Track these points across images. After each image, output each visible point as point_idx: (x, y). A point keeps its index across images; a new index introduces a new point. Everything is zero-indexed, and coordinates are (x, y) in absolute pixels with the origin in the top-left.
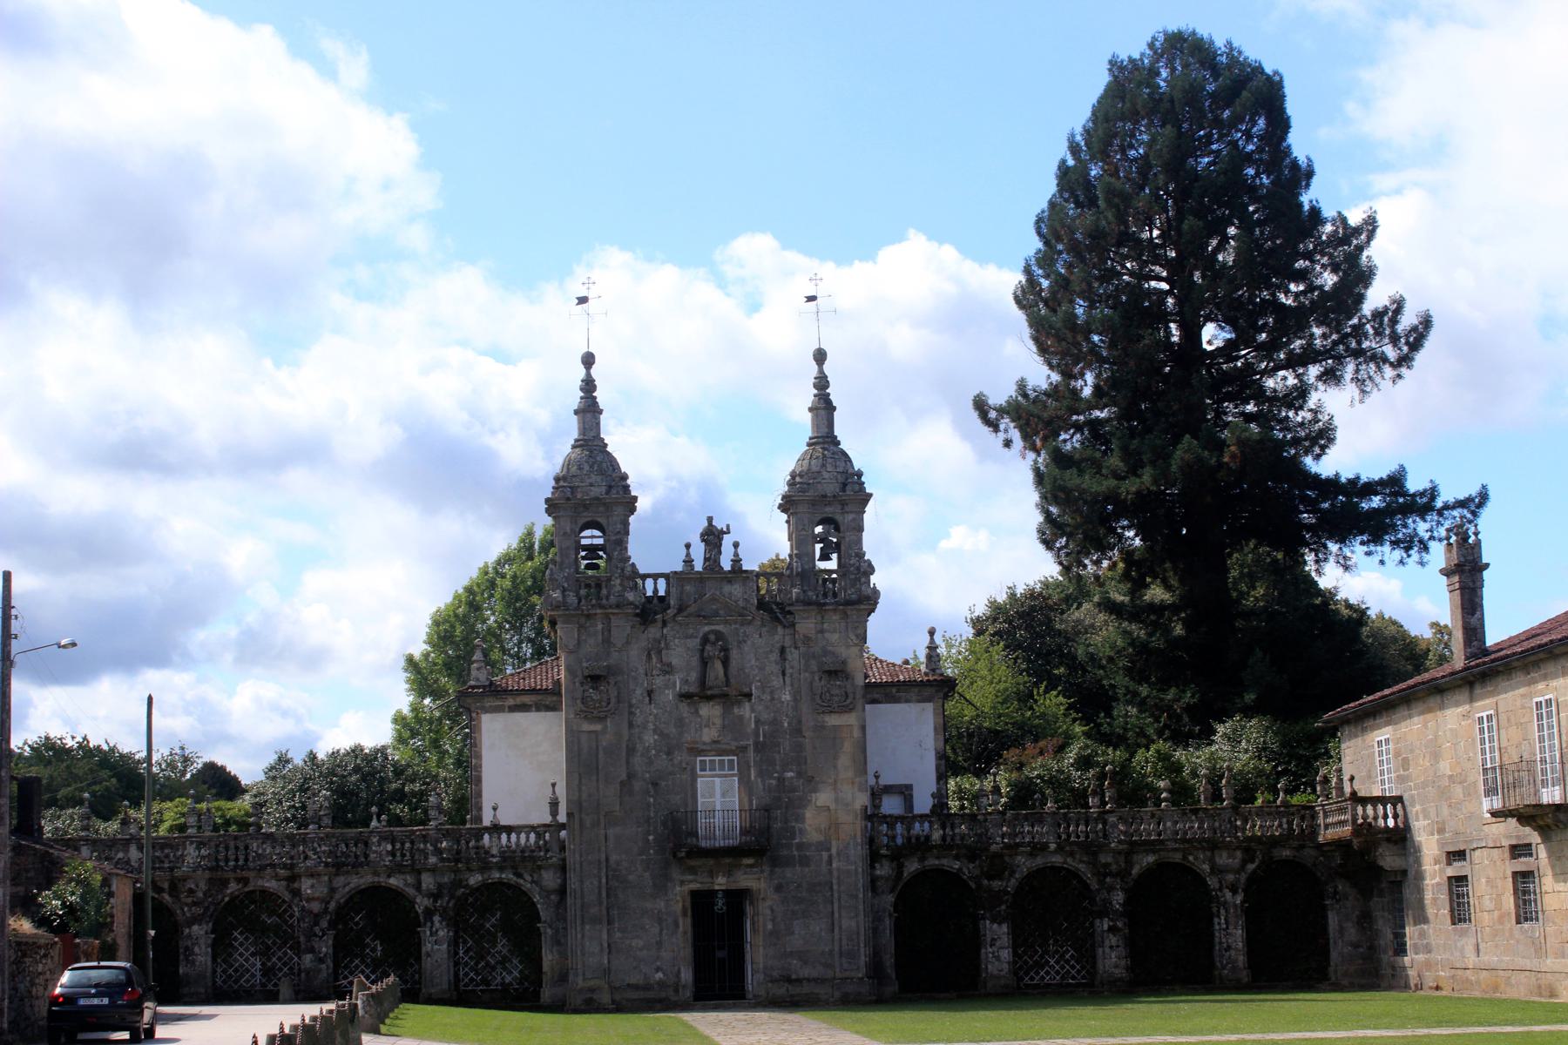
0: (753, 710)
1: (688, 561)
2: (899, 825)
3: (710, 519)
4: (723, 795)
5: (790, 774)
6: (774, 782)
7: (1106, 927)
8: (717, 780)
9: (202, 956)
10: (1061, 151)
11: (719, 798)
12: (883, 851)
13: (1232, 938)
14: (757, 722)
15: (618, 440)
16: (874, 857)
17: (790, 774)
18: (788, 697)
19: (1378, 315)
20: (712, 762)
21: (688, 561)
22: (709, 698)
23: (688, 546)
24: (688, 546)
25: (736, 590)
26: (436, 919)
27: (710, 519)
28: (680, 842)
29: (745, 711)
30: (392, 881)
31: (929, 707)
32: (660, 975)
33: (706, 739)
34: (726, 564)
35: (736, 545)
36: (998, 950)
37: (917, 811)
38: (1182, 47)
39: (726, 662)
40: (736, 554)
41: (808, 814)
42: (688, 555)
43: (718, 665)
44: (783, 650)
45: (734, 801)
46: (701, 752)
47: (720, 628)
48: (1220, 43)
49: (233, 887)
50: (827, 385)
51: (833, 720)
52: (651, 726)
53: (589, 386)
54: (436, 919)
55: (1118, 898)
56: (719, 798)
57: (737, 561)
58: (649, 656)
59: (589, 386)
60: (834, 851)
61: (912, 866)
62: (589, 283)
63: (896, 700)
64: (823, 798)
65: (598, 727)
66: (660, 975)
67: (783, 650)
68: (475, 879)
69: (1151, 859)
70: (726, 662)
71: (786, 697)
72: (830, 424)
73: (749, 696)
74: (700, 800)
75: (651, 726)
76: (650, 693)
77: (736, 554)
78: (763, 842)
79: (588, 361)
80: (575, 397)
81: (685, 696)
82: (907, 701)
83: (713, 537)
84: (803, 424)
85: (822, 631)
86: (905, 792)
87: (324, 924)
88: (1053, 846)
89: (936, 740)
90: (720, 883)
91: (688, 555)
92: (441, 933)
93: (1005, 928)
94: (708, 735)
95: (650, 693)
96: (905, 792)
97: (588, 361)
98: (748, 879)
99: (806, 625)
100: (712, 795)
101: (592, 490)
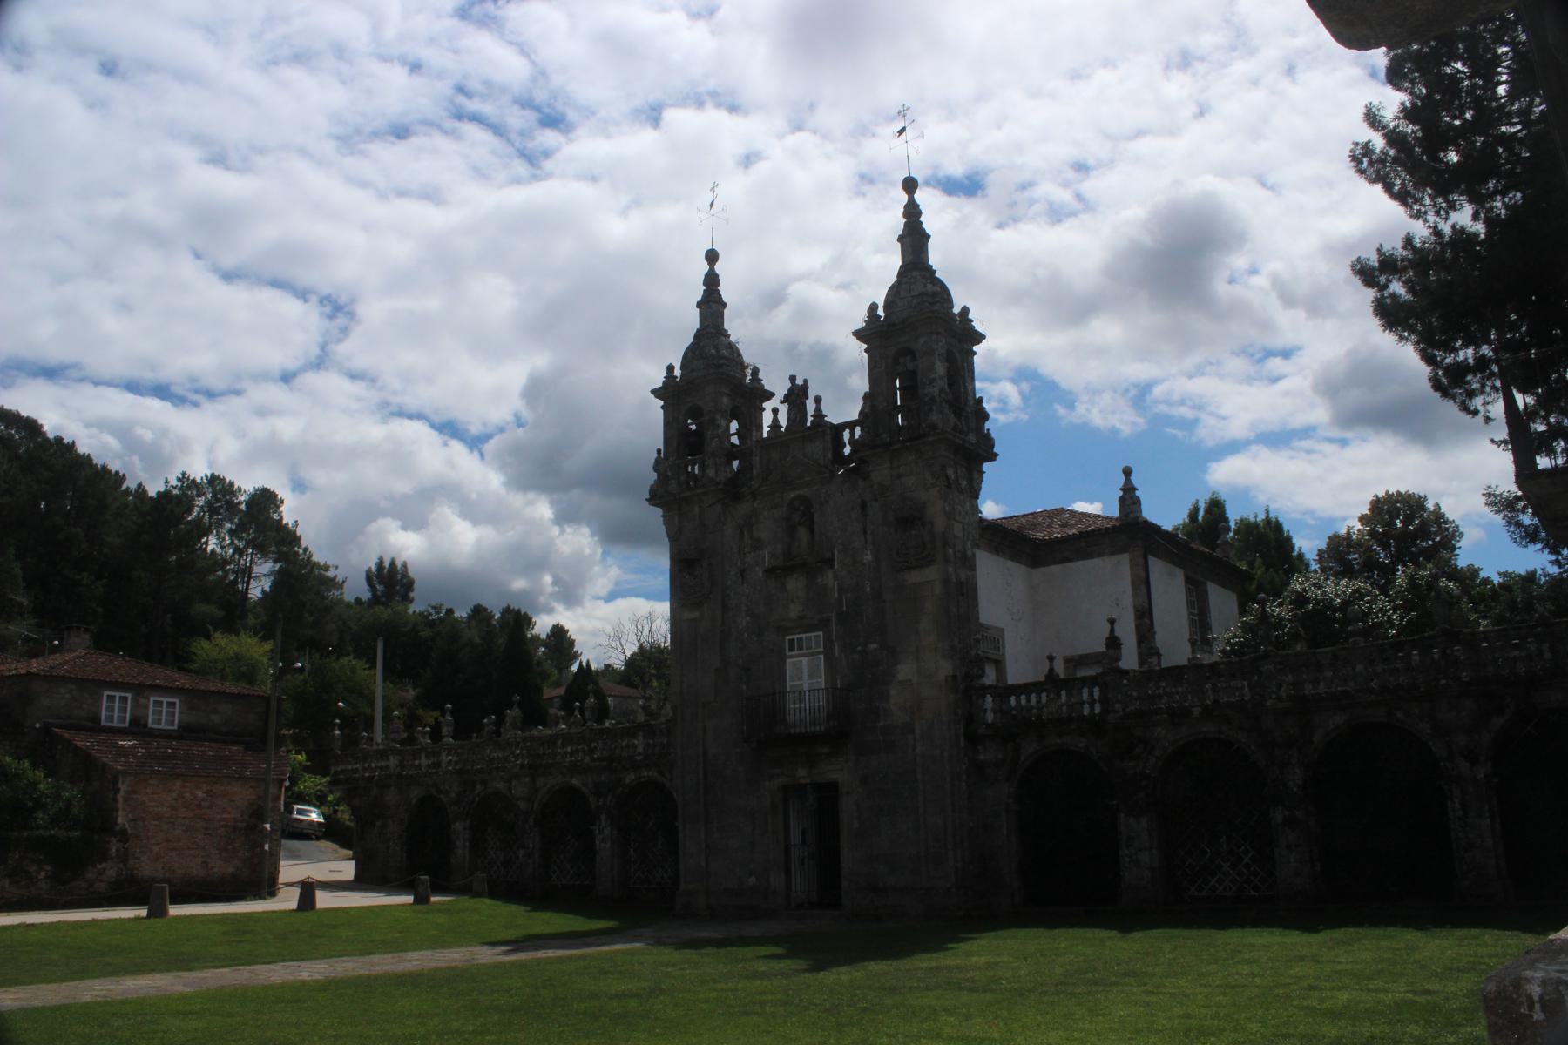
0: (836, 578)
2: (989, 699)
3: (793, 378)
4: (811, 676)
5: (874, 646)
6: (856, 656)
8: (805, 660)
9: (462, 849)
12: (981, 731)
14: (840, 589)
17: (874, 646)
18: (870, 557)
20: (800, 640)
21: (775, 425)
23: (775, 411)
24: (775, 411)
25: (817, 450)
26: (603, 817)
27: (793, 378)
28: (767, 732)
29: (829, 579)
30: (574, 781)
31: (1125, 558)
33: (792, 615)
35: (818, 400)
36: (1140, 851)
39: (812, 531)
40: (818, 411)
41: (893, 692)
42: (775, 420)
43: (803, 534)
44: (864, 506)
45: (821, 682)
46: (786, 631)
49: (479, 788)
50: (919, 214)
51: (913, 577)
52: (744, 608)
53: (712, 281)
54: (603, 817)
57: (819, 415)
58: (742, 533)
59: (712, 281)
60: (917, 732)
63: (1087, 555)
64: (905, 671)
65: (696, 614)
66: (752, 880)
67: (864, 506)
68: (630, 778)
70: (812, 531)
71: (869, 557)
73: (829, 562)
74: (789, 684)
75: (744, 608)
76: (742, 572)
77: (818, 411)
79: (712, 257)
80: (699, 292)
81: (769, 572)
82: (1100, 555)
85: (899, 476)
88: (1197, 711)
89: (1135, 595)
90: (802, 773)
91: (775, 420)
92: (607, 831)
94: (794, 610)
95: (742, 572)
97: (712, 257)
98: (840, 771)
99: (881, 472)
100: (800, 678)
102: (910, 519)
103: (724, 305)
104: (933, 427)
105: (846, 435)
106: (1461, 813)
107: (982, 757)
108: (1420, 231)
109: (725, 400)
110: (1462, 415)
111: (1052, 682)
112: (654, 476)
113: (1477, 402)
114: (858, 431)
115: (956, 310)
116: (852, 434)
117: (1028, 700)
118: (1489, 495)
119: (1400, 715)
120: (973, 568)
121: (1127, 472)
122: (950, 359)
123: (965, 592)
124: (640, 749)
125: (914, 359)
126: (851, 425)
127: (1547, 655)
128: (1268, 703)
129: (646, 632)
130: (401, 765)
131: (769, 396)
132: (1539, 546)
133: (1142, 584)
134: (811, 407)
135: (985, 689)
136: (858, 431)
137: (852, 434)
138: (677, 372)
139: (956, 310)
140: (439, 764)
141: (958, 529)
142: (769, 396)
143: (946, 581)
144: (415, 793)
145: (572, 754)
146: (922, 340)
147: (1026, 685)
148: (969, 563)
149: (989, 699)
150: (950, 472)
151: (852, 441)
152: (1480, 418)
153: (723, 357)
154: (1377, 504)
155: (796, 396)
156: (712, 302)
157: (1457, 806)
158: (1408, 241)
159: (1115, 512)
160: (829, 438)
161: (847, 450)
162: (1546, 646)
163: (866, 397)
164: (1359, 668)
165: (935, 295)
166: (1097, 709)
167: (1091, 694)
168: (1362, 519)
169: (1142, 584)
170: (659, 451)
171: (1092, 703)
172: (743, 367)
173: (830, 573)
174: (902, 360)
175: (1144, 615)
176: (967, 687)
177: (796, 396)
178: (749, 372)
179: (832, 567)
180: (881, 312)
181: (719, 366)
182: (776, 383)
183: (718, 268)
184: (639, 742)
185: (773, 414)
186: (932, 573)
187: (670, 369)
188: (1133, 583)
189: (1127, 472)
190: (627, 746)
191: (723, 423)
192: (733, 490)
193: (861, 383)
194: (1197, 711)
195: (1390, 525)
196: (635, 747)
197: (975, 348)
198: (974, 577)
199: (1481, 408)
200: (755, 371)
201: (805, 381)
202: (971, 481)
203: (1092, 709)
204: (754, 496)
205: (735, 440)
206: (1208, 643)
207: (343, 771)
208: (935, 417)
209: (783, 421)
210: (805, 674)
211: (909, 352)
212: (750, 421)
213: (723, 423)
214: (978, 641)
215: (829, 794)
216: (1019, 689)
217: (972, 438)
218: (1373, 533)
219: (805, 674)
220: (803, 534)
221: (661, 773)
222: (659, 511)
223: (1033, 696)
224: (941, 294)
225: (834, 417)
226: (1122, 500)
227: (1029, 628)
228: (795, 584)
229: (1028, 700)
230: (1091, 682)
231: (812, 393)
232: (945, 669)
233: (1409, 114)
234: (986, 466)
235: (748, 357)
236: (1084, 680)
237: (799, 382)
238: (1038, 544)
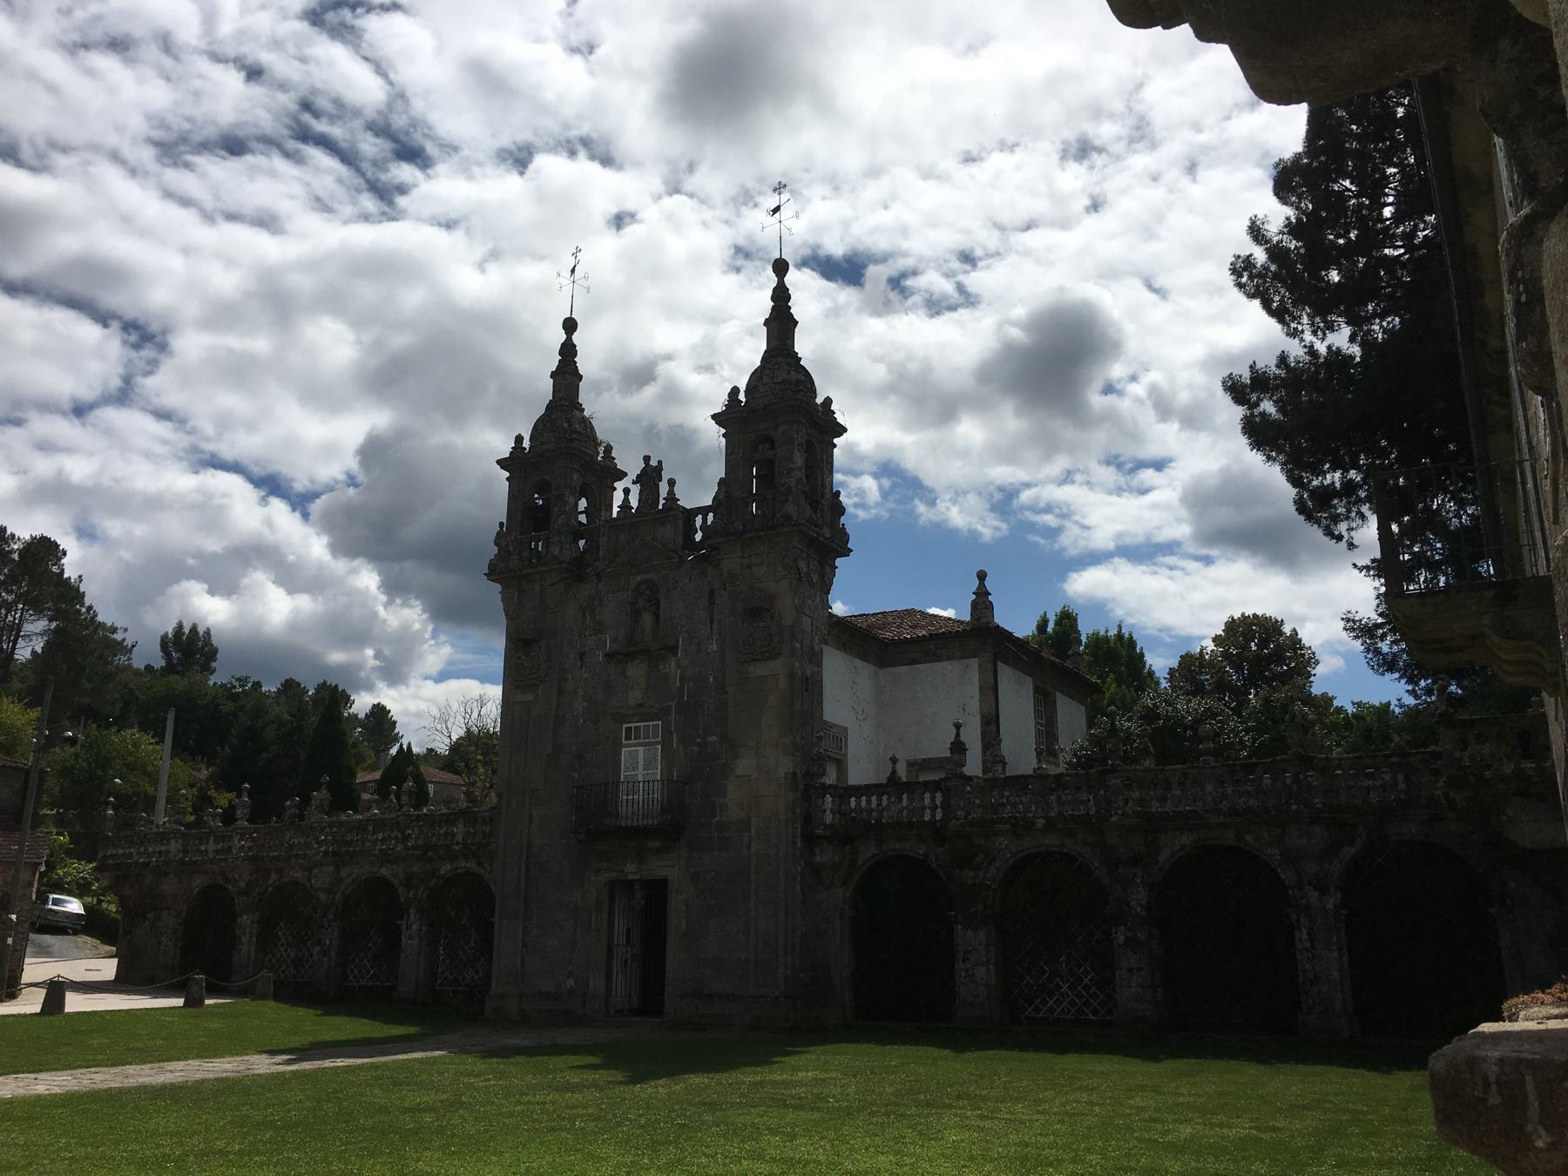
0: (679, 666)
2: (829, 798)
3: (647, 459)
7: (1121, 939)
8: (641, 749)
12: (819, 832)
13: (1324, 962)
14: (682, 680)
15: (584, 397)
16: (810, 840)
18: (715, 647)
21: (625, 505)
22: (630, 656)
24: (627, 491)
25: (668, 533)
28: (597, 825)
29: (671, 667)
30: (384, 871)
31: (974, 663)
32: (571, 982)
33: (631, 702)
35: (672, 483)
36: (976, 968)
39: (657, 616)
40: (671, 493)
43: (647, 618)
44: (712, 594)
45: (658, 774)
46: (625, 718)
47: (652, 576)
51: (758, 670)
53: (568, 351)
54: (412, 911)
55: (1139, 898)
57: (672, 498)
58: (584, 617)
59: (568, 351)
61: (868, 852)
63: (935, 657)
64: (744, 765)
65: (530, 697)
67: (712, 594)
68: (445, 869)
69: (1186, 839)
73: (673, 650)
76: (582, 656)
77: (671, 493)
78: (676, 823)
79: (570, 325)
80: (553, 362)
82: (949, 659)
85: (750, 566)
87: (331, 916)
89: (981, 701)
90: (631, 870)
92: (415, 927)
93: (982, 936)
94: (634, 697)
95: (582, 656)
97: (570, 325)
98: (669, 868)
102: (758, 610)
103: (581, 377)
104: (788, 517)
105: (699, 520)
106: (1308, 944)
107: (818, 859)
108: (1296, 350)
109: (575, 476)
110: (1327, 539)
111: (893, 785)
112: (495, 550)
113: (1342, 527)
114: (711, 517)
115: (819, 400)
116: (705, 520)
117: (869, 802)
118: (1348, 620)
119: (1249, 838)
120: (819, 664)
121: (982, 576)
122: (809, 448)
123: (809, 689)
124: (460, 838)
125: (773, 447)
126: (704, 511)
127: (1402, 786)
128: (1114, 819)
129: (475, 715)
130: (185, 851)
131: (622, 475)
132: (1397, 675)
133: (990, 690)
134: (664, 489)
135: (825, 789)
136: (711, 517)
137: (705, 520)
138: (526, 444)
139: (819, 400)
140: (230, 849)
141: (806, 621)
142: (622, 475)
143: (791, 676)
144: (198, 882)
145: (383, 841)
146: (782, 428)
147: (867, 786)
148: (816, 659)
149: (829, 798)
150: (802, 564)
151: (704, 527)
152: (1343, 544)
153: (575, 431)
154: (1231, 625)
155: (650, 476)
156: (567, 372)
157: (1305, 936)
158: (1283, 359)
159: (967, 618)
160: (680, 523)
161: (698, 536)
162: (1401, 777)
163: (721, 483)
164: (1209, 788)
165: (798, 382)
166: (939, 816)
167: (933, 800)
168: (1216, 639)
169: (990, 690)
170: (501, 524)
171: (934, 808)
172: (597, 443)
173: (673, 661)
174: (760, 447)
175: (991, 722)
176: (807, 785)
177: (650, 476)
178: (601, 449)
179: (675, 654)
180: (742, 397)
181: (572, 440)
182: (630, 463)
183: (575, 338)
184: (459, 830)
185: (624, 495)
186: (777, 667)
187: (519, 439)
188: (981, 689)
189: (982, 576)
190: (446, 834)
191: (571, 499)
192: (578, 570)
193: (718, 470)
194: (1040, 822)
196: (453, 835)
197: (836, 441)
198: (820, 673)
199: (1345, 534)
200: (609, 449)
201: (660, 462)
202: (822, 575)
203: (933, 816)
204: (599, 577)
205: (583, 518)
206: (1052, 753)
207: (112, 856)
208: (791, 509)
209: (634, 503)
210: (641, 764)
211: (770, 441)
212: (601, 500)
213: (571, 499)
214: (820, 738)
215: (657, 891)
216: (858, 791)
217: (827, 532)
218: (1225, 655)
219: (641, 764)
220: (647, 618)
221: (480, 864)
222: (498, 587)
223: (874, 798)
224: (805, 382)
225: (687, 501)
226: (974, 604)
227: (871, 727)
228: (636, 670)
229: (869, 802)
230: (935, 786)
231: (665, 476)
233: (1292, 229)
234: (839, 561)
235: (601, 434)
236: (926, 784)
237: (653, 463)
238: (889, 644)
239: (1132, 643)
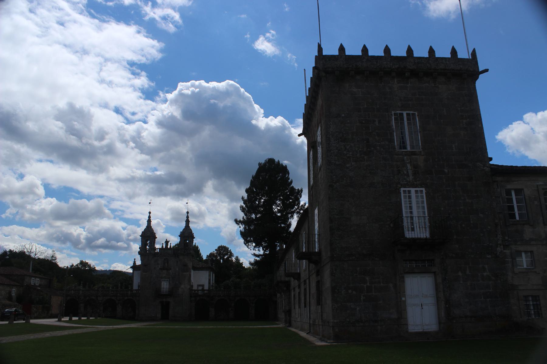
1: (163, 246)
10: (251, 178)
11: (165, 286)
19: (302, 205)
21: (163, 246)
34: (169, 247)
37: (205, 289)
38: (271, 161)
43: (166, 264)
48: (276, 160)
51: (185, 273)
53: (149, 217)
56: (165, 286)
59: (149, 217)
62: (151, 200)
64: (182, 286)
68: (126, 298)
72: (189, 224)
79: (150, 213)
81: (160, 269)
83: (167, 242)
84: (184, 224)
86: (203, 286)
96: (203, 286)
97: (150, 213)
101: (148, 235)
133: (210, 275)
148: (191, 272)
154: (219, 247)
156: (149, 221)
168: (216, 250)
195: (220, 252)
218: (217, 253)
232: (189, 287)
239: (197, 247)
